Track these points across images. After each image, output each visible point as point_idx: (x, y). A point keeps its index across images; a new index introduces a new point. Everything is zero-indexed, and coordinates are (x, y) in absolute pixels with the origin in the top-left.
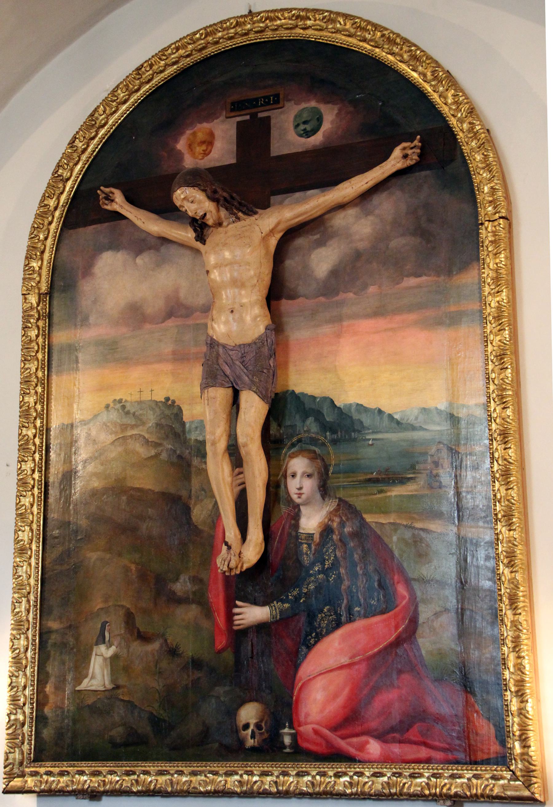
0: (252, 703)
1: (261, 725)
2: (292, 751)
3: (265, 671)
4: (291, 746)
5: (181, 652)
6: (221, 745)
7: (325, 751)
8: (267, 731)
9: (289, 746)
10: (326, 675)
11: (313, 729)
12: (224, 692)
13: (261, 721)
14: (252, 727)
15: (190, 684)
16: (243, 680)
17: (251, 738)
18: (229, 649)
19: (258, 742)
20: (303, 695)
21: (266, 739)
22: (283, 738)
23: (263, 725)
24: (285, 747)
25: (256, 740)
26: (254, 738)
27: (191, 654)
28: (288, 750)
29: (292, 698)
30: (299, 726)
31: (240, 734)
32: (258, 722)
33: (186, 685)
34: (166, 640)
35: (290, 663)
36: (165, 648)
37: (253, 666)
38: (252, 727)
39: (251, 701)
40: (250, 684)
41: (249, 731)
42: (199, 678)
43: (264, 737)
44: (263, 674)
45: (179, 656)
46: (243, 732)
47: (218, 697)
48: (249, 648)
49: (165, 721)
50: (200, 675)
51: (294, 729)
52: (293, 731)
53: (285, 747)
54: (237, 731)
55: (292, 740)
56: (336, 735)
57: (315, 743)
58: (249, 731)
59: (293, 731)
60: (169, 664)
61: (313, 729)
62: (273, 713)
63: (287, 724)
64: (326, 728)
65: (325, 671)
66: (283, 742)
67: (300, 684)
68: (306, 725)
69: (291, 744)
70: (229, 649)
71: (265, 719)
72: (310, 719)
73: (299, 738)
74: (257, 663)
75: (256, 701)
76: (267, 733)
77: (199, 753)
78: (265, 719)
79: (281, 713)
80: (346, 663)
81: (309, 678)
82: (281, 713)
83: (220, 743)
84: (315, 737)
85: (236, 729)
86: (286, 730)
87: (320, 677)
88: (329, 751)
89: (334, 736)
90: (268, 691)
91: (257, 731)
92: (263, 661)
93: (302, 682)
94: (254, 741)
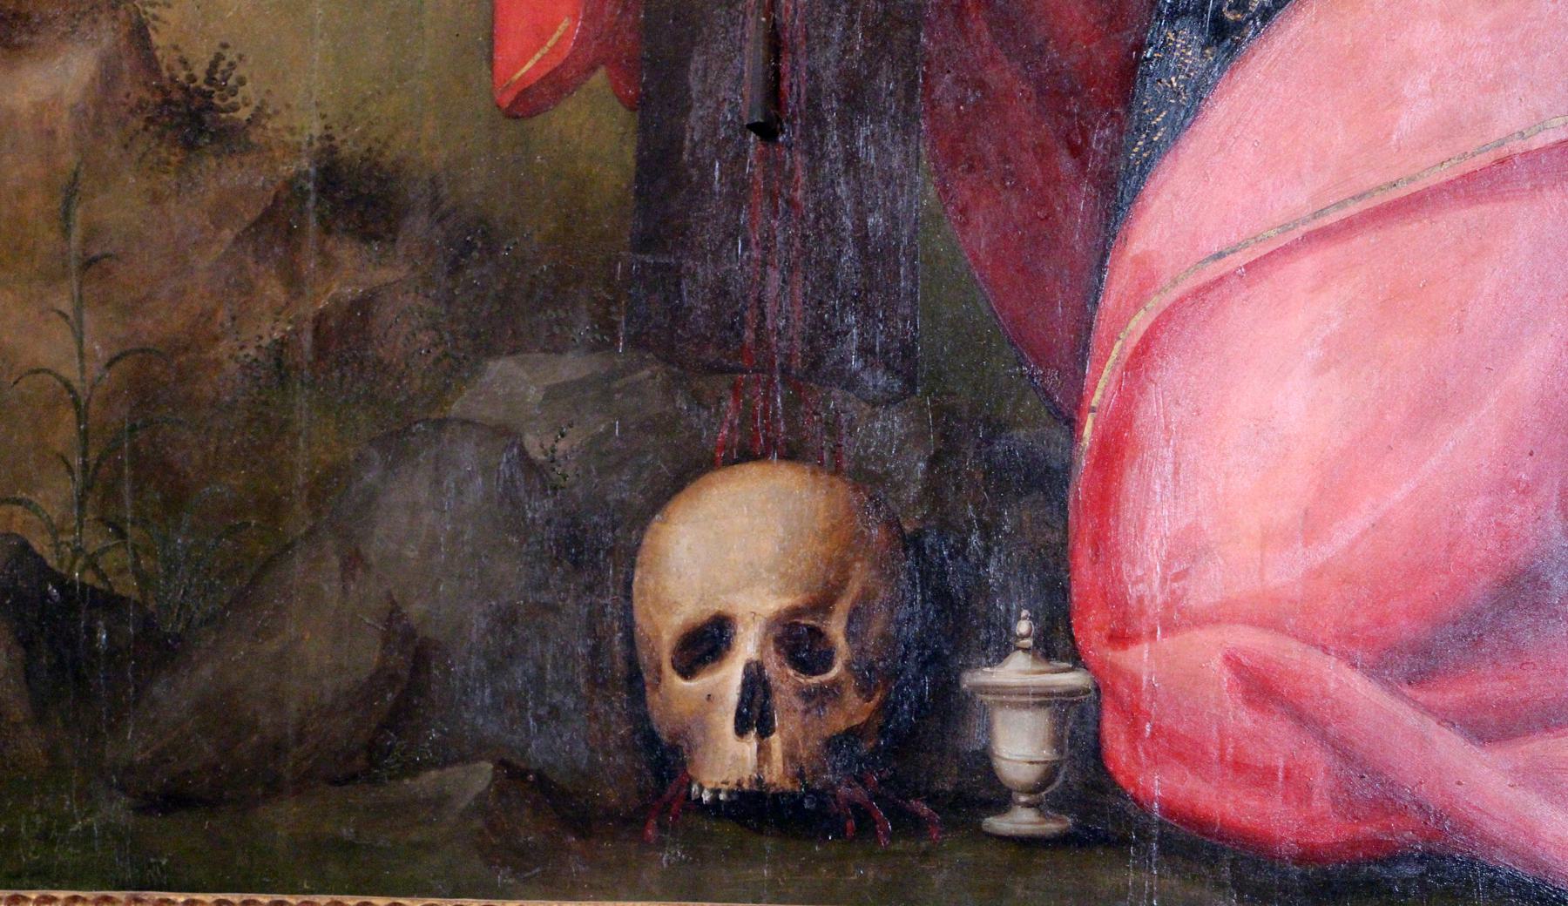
0: (753, 469)
1: (817, 634)
2: (1052, 827)
3: (862, 238)
4: (1043, 792)
5: (244, 114)
6: (511, 773)
7: (1330, 833)
8: (866, 677)
9: (1033, 790)
10: (1363, 242)
11: (1232, 661)
12: (552, 394)
13: (822, 604)
14: (747, 646)
15: (307, 340)
16: (697, 303)
17: (741, 729)
18: (600, 78)
19: (790, 756)
20: (1153, 409)
21: (853, 734)
22: (988, 729)
23: (836, 628)
24: (1001, 800)
25: (776, 741)
26: (765, 730)
27: (316, 128)
28: (1021, 821)
29: (1071, 424)
30: (1121, 638)
31: (653, 698)
32: (795, 612)
33: (282, 344)
34: (140, 33)
35: (1066, 164)
36: (131, 89)
37: (773, 196)
38: (747, 646)
39: (746, 454)
40: (749, 335)
41: (728, 678)
42: (363, 307)
43: (838, 721)
44: (850, 252)
45: (231, 139)
46: (679, 683)
47: (505, 433)
48: (751, 60)
49: (111, 603)
50: (386, 275)
51: (1076, 659)
52: (1073, 679)
53: (1001, 800)
54: (635, 681)
55: (1057, 742)
56: (1428, 709)
57: (1239, 766)
58: (728, 678)
59: (1073, 679)
60: (156, 198)
61: (1232, 661)
62: (913, 542)
63: (1023, 627)
64: (1344, 656)
65: (1354, 209)
66: (984, 760)
67: (1139, 323)
68: (1170, 628)
69: (1050, 773)
70: (600, 78)
71: (854, 587)
72: (1204, 592)
73: (1113, 727)
74: (802, 176)
75: (792, 454)
76: (865, 690)
77: (347, 832)
78: (854, 587)
79: (975, 540)
80: (1538, 142)
81: (1212, 271)
82: (975, 540)
83: (502, 763)
84: (1244, 719)
85: (632, 661)
86: (1017, 670)
87: (1307, 265)
88: (1368, 830)
89: (1411, 718)
90: (878, 380)
91: (784, 679)
92: (851, 159)
93: (1156, 304)
94: (763, 752)
